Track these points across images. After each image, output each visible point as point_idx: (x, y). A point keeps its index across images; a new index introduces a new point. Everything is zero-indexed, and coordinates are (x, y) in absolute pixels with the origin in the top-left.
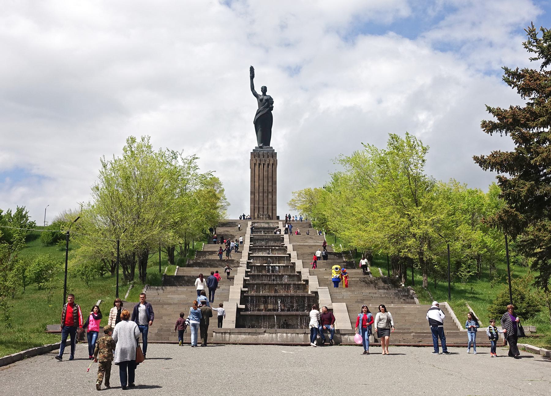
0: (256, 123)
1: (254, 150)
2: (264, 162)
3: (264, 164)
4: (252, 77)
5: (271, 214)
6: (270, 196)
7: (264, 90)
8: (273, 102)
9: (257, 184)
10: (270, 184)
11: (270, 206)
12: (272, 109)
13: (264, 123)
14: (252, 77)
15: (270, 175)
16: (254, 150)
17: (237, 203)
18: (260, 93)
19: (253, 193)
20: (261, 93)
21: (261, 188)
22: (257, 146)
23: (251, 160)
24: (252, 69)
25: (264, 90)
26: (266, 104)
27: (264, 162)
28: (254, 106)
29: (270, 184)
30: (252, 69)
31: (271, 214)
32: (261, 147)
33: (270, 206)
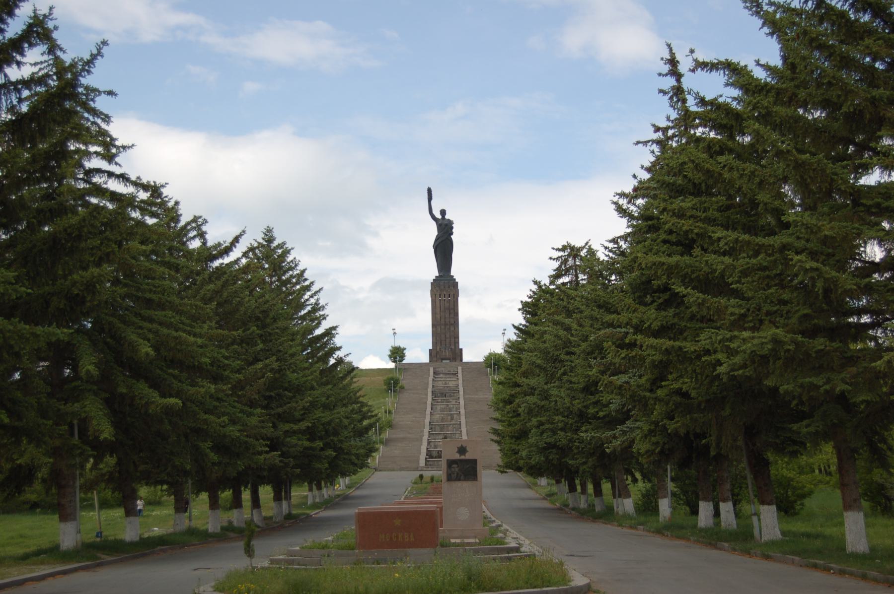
2: (445, 292)
4: (430, 198)
6: (452, 329)
7: (443, 212)
8: (452, 228)
9: (438, 316)
10: (452, 316)
11: (453, 340)
12: (452, 234)
13: (443, 249)
14: (430, 198)
15: (452, 306)
18: (439, 216)
19: (433, 326)
21: (443, 320)
23: (431, 291)
24: (429, 191)
25: (443, 212)
26: (445, 229)
27: (445, 292)
29: (452, 316)
30: (429, 191)
32: (440, 276)
33: (453, 340)
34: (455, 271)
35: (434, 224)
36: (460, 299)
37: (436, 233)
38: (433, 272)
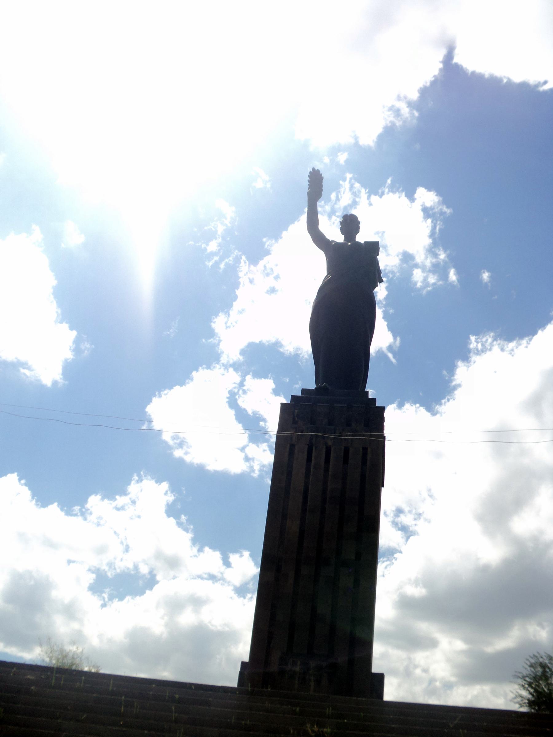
7: (350, 225)
9: (293, 526)
18: (336, 235)
20: (339, 238)
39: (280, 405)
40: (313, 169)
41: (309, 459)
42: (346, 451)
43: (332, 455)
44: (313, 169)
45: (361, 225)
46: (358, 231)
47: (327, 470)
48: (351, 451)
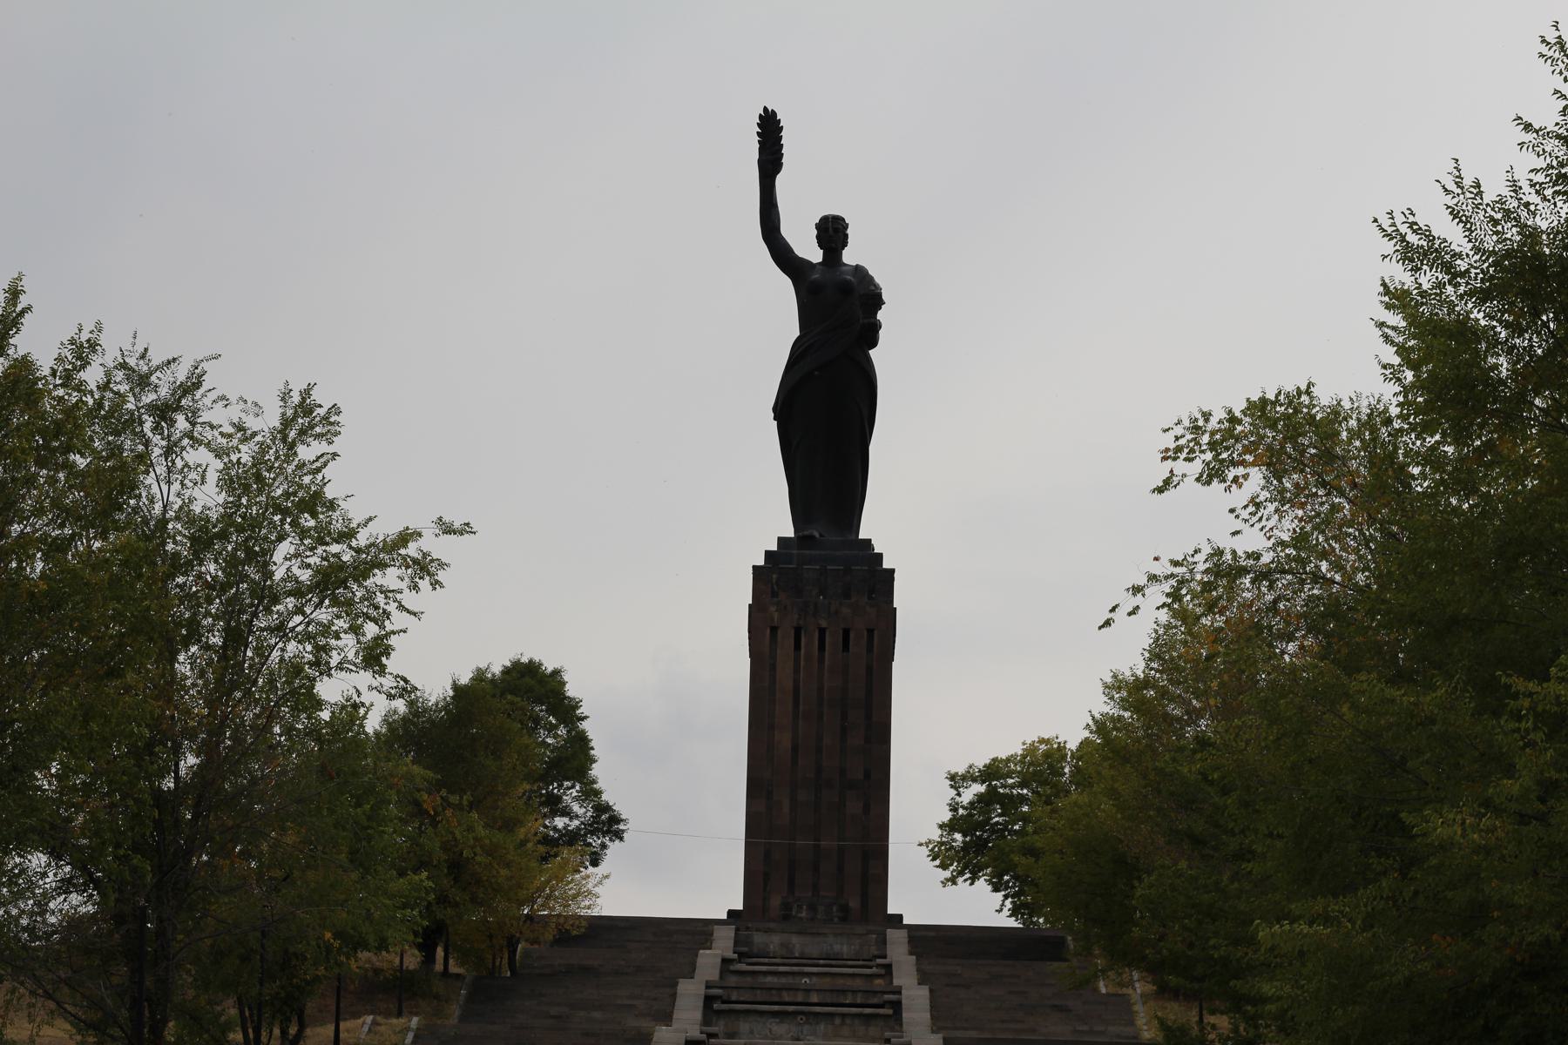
0: (785, 410)
1: (768, 554)
2: (824, 622)
3: (822, 631)
5: (854, 904)
7: (832, 232)
8: (874, 300)
12: (871, 335)
13: (827, 409)
16: (768, 554)
17: (674, 846)
18: (809, 250)
20: (815, 255)
22: (789, 532)
24: (770, 127)
25: (832, 232)
27: (824, 622)
28: (774, 319)
30: (770, 127)
31: (854, 904)
34: (879, 523)
35: (784, 288)
36: (896, 666)
37: (791, 330)
38: (767, 516)
39: (751, 570)
40: (765, 109)
41: (797, 647)
42: (846, 633)
43: (828, 639)
44: (765, 109)
45: (849, 231)
46: (845, 244)
47: (821, 660)
48: (852, 635)
